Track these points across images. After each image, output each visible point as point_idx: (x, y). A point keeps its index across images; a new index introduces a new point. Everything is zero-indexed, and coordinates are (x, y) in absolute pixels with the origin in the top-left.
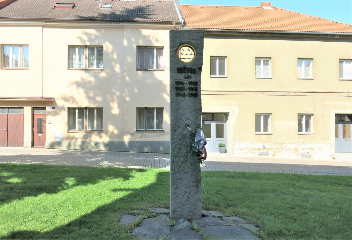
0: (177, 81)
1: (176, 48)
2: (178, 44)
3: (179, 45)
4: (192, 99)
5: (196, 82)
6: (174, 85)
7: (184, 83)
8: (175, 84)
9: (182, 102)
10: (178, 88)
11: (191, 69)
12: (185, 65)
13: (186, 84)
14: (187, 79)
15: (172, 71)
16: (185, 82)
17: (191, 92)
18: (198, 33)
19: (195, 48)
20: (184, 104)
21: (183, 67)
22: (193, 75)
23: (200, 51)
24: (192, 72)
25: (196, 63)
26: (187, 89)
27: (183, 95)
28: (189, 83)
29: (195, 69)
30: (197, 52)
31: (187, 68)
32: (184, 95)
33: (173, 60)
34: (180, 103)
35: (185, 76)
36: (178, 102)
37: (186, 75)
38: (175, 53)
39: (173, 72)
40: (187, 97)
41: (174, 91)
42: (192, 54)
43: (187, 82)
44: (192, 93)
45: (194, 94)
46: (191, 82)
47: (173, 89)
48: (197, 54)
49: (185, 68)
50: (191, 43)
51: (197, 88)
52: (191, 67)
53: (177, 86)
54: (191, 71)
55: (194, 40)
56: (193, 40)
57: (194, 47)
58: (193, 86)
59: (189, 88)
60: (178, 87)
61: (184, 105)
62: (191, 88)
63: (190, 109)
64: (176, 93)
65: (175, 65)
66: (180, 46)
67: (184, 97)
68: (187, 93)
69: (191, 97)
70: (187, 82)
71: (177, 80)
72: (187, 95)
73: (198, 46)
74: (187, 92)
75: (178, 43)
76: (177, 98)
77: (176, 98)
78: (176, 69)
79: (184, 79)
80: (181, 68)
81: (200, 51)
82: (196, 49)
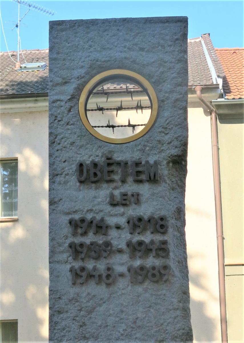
0: (77, 217)
1: (74, 86)
3: (86, 73)
4: (146, 290)
5: (162, 219)
6: (66, 237)
7: (108, 227)
8: (67, 230)
9: (100, 305)
10: (79, 249)
11: (137, 164)
12: (110, 152)
13: (118, 227)
14: (121, 209)
16: (112, 221)
17: (138, 263)
18: (161, 25)
19: (153, 80)
20: (110, 315)
21: (103, 159)
22: (145, 189)
23: (171, 92)
24: (143, 177)
25: (159, 141)
26: (120, 251)
27: (104, 275)
29: (156, 163)
31: (119, 164)
33: (60, 134)
34: (90, 312)
35: (112, 196)
36: (80, 310)
37: (117, 193)
38: (69, 105)
40: (122, 283)
43: (122, 221)
44: (142, 268)
45: (154, 268)
46: (140, 219)
49: (110, 163)
50: (134, 62)
52: (136, 156)
53: (78, 240)
54: (139, 173)
55: (148, 51)
56: (142, 49)
57: (149, 77)
58: (147, 238)
59: (129, 244)
60: (82, 245)
61: (111, 320)
62: (141, 243)
63: (138, 335)
66: (92, 77)
67: (108, 285)
68: (123, 269)
69: (141, 283)
70: (122, 221)
71: (75, 212)
72: (122, 275)
73: (163, 73)
74: (122, 264)
75: (82, 67)
76: (77, 289)
77: (72, 291)
78: (74, 167)
79: (109, 208)
80: (95, 165)
81: (171, 92)
82: (156, 84)
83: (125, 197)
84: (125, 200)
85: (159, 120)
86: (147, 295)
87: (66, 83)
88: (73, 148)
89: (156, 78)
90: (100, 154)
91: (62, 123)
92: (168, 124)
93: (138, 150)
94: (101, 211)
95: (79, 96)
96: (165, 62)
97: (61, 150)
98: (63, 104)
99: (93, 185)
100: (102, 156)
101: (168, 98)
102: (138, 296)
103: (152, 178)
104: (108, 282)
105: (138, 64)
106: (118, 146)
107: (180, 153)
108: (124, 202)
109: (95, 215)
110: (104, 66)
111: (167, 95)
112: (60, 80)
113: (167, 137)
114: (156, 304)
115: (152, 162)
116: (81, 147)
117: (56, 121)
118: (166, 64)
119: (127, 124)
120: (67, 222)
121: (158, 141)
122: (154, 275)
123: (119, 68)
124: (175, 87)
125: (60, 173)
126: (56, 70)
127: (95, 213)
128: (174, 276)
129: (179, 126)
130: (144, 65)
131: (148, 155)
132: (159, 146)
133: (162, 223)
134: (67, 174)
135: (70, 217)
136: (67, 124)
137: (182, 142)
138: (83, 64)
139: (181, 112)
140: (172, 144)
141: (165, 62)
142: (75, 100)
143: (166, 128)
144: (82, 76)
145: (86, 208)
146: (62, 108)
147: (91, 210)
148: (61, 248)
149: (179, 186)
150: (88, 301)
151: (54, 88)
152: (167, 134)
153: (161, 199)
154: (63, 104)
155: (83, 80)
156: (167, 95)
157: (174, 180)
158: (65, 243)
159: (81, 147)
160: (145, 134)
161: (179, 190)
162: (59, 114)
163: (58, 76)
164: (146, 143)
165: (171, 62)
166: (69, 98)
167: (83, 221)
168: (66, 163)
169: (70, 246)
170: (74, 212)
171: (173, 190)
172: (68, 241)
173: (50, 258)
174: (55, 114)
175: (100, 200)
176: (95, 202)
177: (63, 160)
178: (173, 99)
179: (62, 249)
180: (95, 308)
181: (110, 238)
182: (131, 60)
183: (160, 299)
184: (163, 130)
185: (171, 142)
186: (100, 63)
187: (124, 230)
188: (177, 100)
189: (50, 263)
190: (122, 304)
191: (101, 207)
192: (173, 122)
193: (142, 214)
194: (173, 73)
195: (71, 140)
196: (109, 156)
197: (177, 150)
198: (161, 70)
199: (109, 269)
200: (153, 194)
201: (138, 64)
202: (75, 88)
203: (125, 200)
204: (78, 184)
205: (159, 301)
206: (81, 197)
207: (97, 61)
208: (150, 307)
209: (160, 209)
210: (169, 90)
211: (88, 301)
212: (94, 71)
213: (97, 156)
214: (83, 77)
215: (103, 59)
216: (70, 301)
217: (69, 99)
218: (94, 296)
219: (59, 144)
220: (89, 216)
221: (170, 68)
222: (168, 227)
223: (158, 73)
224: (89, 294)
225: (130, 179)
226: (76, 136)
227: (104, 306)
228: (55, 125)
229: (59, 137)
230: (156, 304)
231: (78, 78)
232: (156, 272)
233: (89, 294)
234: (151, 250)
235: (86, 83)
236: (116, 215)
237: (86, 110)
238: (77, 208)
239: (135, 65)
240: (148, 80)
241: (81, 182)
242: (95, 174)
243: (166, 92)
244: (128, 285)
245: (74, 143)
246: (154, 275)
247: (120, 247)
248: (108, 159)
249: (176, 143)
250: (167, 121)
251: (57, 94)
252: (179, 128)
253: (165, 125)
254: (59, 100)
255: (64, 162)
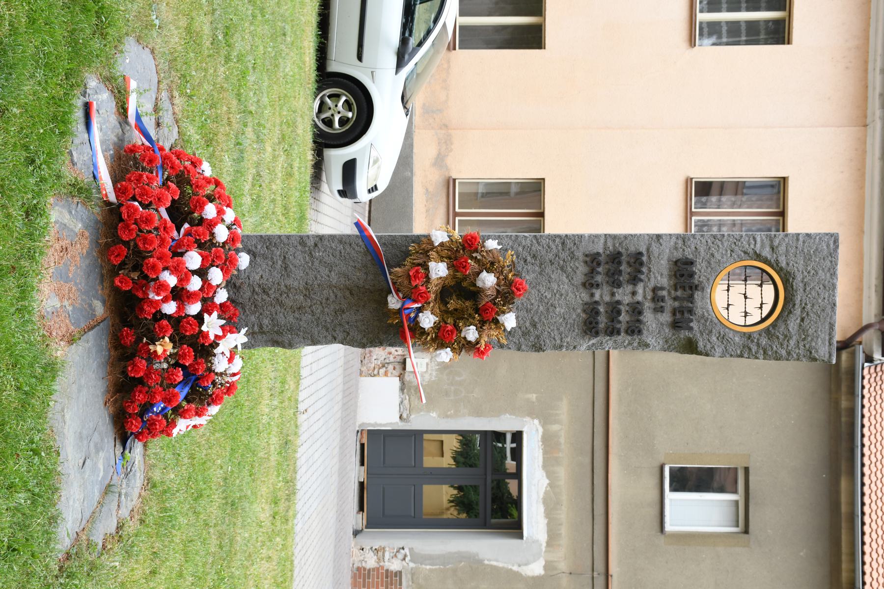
0: (645, 259)
1: (769, 257)
2: (784, 265)
3: (781, 269)
4: (578, 315)
5: (640, 332)
6: (627, 250)
7: (635, 285)
8: (632, 249)
9: (567, 277)
11: (691, 311)
12: (703, 289)
13: (634, 293)
14: (649, 296)
15: (680, 242)
16: (640, 289)
17: (601, 309)
18: (827, 338)
19: (771, 329)
20: (559, 286)
21: (696, 282)
22: (666, 317)
23: (758, 345)
24: (678, 316)
25: (711, 332)
26: (613, 294)
27: (593, 282)
28: (638, 303)
29: (691, 329)
30: (756, 336)
31: (691, 298)
32: (592, 285)
33: (722, 244)
34: (562, 269)
35: (662, 289)
36: (564, 260)
37: (665, 293)
38: (750, 251)
39: (676, 243)
40: (585, 296)
41: (605, 249)
42: (745, 317)
43: (639, 297)
44: (597, 313)
45: (597, 323)
46: (640, 313)
47: (614, 246)
48: (744, 333)
49: (694, 288)
50: (790, 312)
51: (619, 333)
52: (699, 312)
53: (624, 258)
54: (682, 313)
55: (800, 325)
56: (802, 320)
57: (774, 325)
58: (624, 317)
59: (618, 302)
60: (620, 263)
61: (554, 286)
62: (619, 313)
63: (541, 308)
64: (598, 254)
65: (703, 253)
66: (778, 273)
68: (597, 297)
69: (584, 311)
70: (639, 297)
72: (592, 295)
73: (778, 338)
74: (601, 296)
75: (788, 264)
76: (581, 258)
77: (579, 254)
78: (691, 257)
79: (651, 285)
80: (692, 275)
81: (758, 345)
82: (767, 330)
83: (660, 300)
84: (658, 300)
85: (732, 332)
86: (574, 316)
87: (773, 249)
88: (708, 256)
89: (773, 331)
90: (701, 280)
91: (733, 246)
92: (728, 340)
93: (703, 312)
94: (649, 280)
95: (759, 261)
96: (788, 341)
97: (707, 245)
98: (752, 246)
99: (673, 273)
100: (699, 281)
101: (752, 341)
102: (573, 309)
103: (677, 325)
104: (587, 284)
105: (787, 316)
106: (709, 296)
107: (699, 349)
108: (656, 299)
109: (645, 274)
110: (788, 285)
111: (756, 341)
112: (776, 243)
113: (714, 338)
114: (567, 323)
115: (691, 324)
116: (709, 263)
117: (736, 241)
118: (786, 341)
119: (729, 303)
120: (641, 250)
121: (711, 330)
122: (591, 323)
123: (785, 298)
124: (762, 348)
125: (686, 244)
126: (787, 240)
127: (648, 274)
128: (590, 339)
129: (725, 350)
130: (786, 321)
131: (699, 322)
132: (707, 332)
133: (636, 331)
134: (684, 250)
135: (645, 253)
136: (731, 251)
137: (709, 352)
138: (791, 265)
139: (739, 352)
140: (708, 342)
141: (788, 341)
142: (755, 257)
143: (723, 338)
144: (779, 264)
145: (652, 267)
146: (748, 246)
147: (650, 271)
148: (618, 244)
149: (669, 346)
150: (571, 267)
151: (768, 238)
152: (718, 339)
153: (657, 331)
154: (752, 246)
155: (775, 265)
156: (756, 341)
157: (675, 342)
158: (622, 248)
159: (709, 263)
160: (718, 320)
161: (666, 346)
162: (742, 243)
163: (780, 242)
164: (710, 320)
165: (787, 346)
166: (758, 252)
167: (642, 264)
168: (694, 249)
169: (619, 253)
170: (649, 256)
171: (666, 341)
172: (623, 251)
173: (609, 235)
174: (743, 239)
175: (659, 278)
176: (657, 275)
177: (697, 247)
178: (752, 346)
179: (617, 245)
180: (565, 272)
181: (625, 286)
182: (792, 310)
183: (571, 327)
184: (722, 335)
185: (709, 342)
186: (791, 281)
187: (631, 299)
188: (750, 349)
189: (605, 235)
190: (567, 295)
191: (652, 280)
192: (729, 345)
193: (645, 314)
194: (776, 347)
195: (716, 254)
196: (699, 288)
197: (702, 347)
198: (781, 337)
199: (598, 285)
200: (662, 324)
201: (787, 316)
202: (766, 258)
203: (658, 300)
204: (674, 260)
205: (569, 326)
206: (662, 262)
207: (793, 278)
208: (564, 319)
209: (648, 330)
210: (760, 342)
211: (571, 267)
212: (783, 275)
213: (700, 277)
214: (777, 265)
215: (794, 284)
216: (572, 253)
217: (756, 252)
218: (575, 272)
219: (713, 243)
220: (644, 269)
221: (782, 345)
222: (632, 336)
223: (778, 334)
224: (577, 268)
225: (677, 304)
226: (720, 258)
227: (566, 281)
228: (731, 240)
229: (719, 243)
230: (567, 323)
231: (777, 260)
232: (594, 324)
233: (577, 268)
234: (613, 321)
235: (772, 267)
236: (644, 291)
237: (746, 267)
238: (652, 258)
239: (786, 313)
240: (771, 325)
241: (676, 262)
242: (682, 276)
243: (758, 340)
244: (583, 301)
245: (713, 256)
246: (591, 323)
247: (617, 295)
248: (696, 287)
249: (709, 346)
250: (730, 340)
251: (762, 241)
252: (723, 349)
253: (727, 337)
254: (755, 243)
255: (695, 248)
